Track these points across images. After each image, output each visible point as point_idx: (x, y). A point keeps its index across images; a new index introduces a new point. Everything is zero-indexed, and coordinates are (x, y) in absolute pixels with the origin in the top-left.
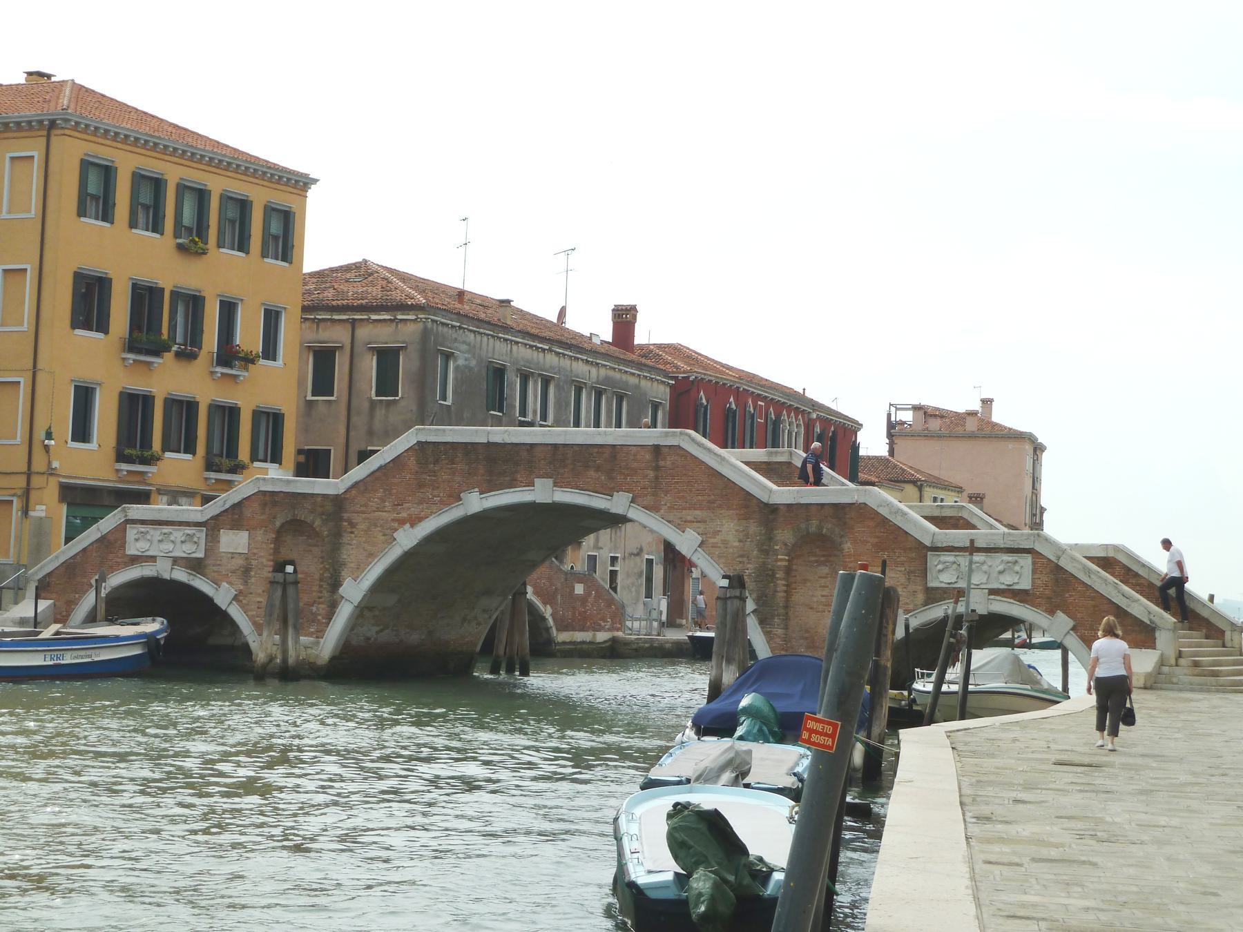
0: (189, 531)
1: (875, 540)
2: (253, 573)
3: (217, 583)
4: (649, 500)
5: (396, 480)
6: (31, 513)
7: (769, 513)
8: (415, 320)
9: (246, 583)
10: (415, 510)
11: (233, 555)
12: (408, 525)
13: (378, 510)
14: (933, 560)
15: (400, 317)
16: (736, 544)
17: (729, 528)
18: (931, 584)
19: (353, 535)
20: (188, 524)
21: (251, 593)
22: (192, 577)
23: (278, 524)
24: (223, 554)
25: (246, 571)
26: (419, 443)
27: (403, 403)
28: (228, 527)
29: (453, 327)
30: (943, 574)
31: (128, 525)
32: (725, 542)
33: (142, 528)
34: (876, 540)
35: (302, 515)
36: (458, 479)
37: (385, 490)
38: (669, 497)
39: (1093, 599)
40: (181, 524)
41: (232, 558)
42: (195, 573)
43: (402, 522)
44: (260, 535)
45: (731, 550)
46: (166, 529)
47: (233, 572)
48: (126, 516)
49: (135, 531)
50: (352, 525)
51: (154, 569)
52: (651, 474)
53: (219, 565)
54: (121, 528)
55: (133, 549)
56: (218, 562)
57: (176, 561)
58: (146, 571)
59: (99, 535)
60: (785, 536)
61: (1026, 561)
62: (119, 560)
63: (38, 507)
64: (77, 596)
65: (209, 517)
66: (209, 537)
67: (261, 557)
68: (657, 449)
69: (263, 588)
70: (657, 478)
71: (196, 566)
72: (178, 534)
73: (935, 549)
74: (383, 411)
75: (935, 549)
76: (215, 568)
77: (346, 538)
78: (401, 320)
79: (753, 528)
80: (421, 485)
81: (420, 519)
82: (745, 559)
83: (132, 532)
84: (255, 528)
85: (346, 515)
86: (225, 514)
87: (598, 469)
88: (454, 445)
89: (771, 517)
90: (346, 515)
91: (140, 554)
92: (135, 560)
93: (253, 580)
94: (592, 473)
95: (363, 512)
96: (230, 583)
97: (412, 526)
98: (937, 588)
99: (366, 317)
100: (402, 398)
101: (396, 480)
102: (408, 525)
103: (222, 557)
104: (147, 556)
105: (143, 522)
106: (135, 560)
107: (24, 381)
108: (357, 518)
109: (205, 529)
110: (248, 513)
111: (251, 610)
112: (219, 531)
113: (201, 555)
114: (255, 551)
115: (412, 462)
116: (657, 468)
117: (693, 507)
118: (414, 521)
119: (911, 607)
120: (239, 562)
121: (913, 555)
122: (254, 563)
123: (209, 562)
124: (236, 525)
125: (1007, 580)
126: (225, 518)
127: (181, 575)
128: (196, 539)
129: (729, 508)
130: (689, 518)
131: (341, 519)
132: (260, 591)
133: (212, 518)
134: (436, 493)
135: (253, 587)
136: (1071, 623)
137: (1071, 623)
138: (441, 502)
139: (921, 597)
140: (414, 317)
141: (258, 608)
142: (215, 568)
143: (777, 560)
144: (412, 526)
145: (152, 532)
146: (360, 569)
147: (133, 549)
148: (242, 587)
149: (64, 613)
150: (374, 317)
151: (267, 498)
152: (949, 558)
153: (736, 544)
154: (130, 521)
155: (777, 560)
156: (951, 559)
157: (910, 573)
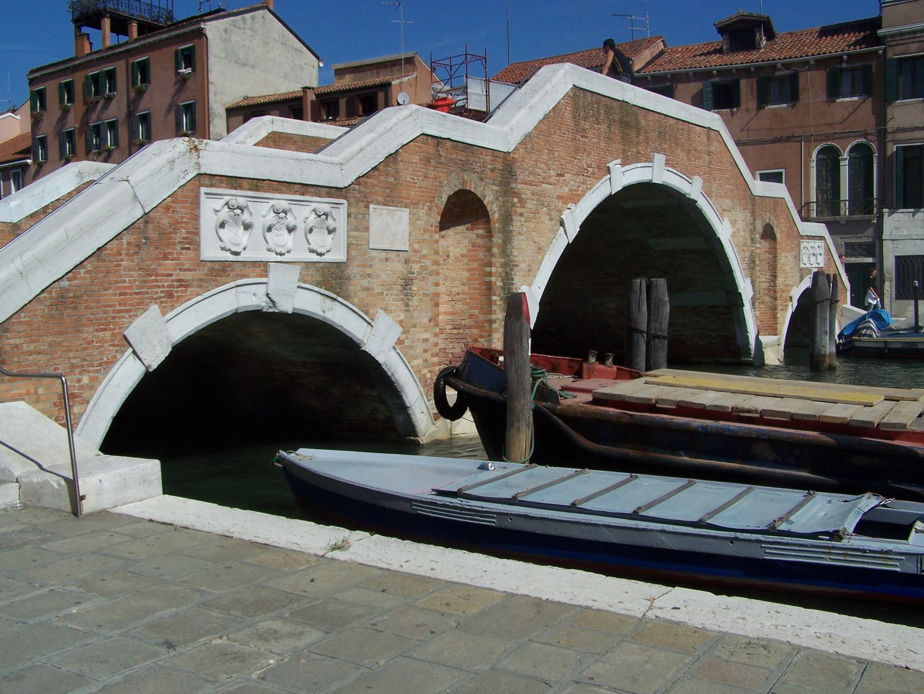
3: (366, 314)
19: (523, 219)
21: (414, 326)
31: (203, 190)
33: (239, 197)
41: (387, 260)
42: (334, 296)
46: (281, 201)
49: (218, 204)
51: (262, 290)
53: (369, 275)
55: (210, 251)
56: (369, 271)
59: (139, 213)
64: (85, 380)
67: (424, 256)
76: (365, 283)
80: (577, 150)
91: (229, 257)
103: (373, 259)
104: (244, 263)
105: (234, 182)
109: (345, 201)
112: (367, 207)
113: (341, 257)
116: (709, 153)
118: (575, 198)
122: (416, 267)
124: (391, 199)
126: (374, 181)
142: (365, 283)
147: (210, 251)
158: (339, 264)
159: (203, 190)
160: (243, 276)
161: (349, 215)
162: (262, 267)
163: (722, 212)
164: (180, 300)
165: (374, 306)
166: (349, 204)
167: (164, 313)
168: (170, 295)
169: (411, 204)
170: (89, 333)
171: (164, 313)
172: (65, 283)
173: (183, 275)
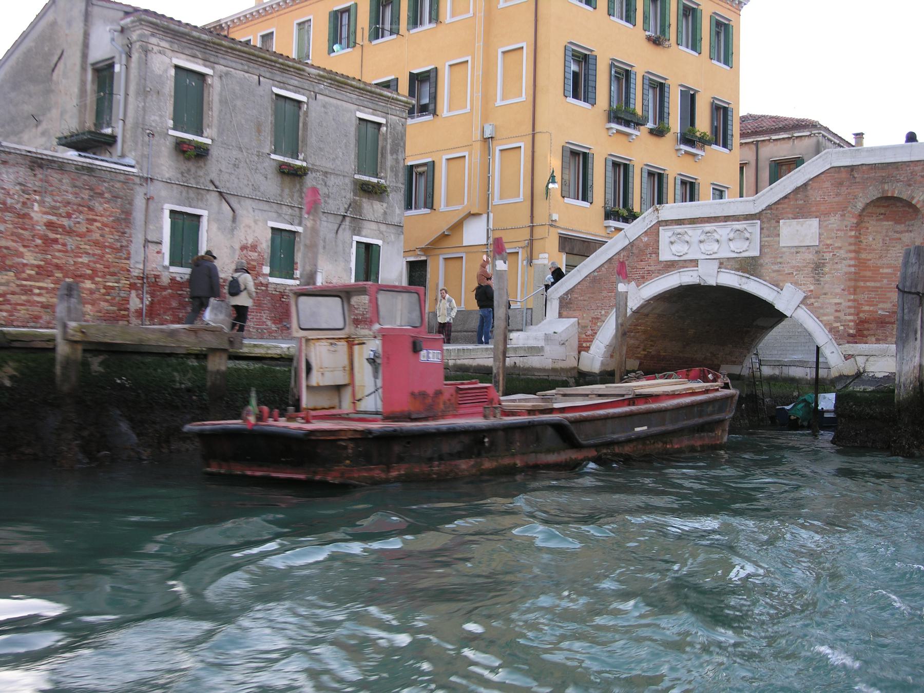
2: (826, 269)
6: (535, 262)
9: (818, 282)
11: (797, 250)
15: (796, 135)
21: (825, 294)
22: (744, 280)
23: (860, 206)
24: (784, 249)
25: (818, 268)
28: (790, 216)
29: (835, 143)
31: (660, 228)
33: (678, 229)
35: (897, 190)
40: (727, 219)
41: (797, 253)
42: (748, 276)
44: (834, 221)
46: (708, 227)
47: (798, 269)
48: (658, 217)
49: (670, 234)
51: (695, 274)
53: (780, 263)
54: (653, 232)
55: (665, 255)
56: (779, 260)
57: (723, 264)
58: (687, 278)
59: (627, 242)
62: (652, 268)
63: (541, 256)
64: (603, 312)
65: (764, 207)
66: (765, 231)
69: (842, 287)
71: (749, 266)
72: (723, 231)
78: (797, 137)
83: (665, 235)
84: (827, 214)
86: (786, 200)
91: (677, 258)
92: (671, 266)
96: (796, 284)
99: (768, 138)
103: (784, 253)
104: (685, 261)
105: (680, 222)
106: (671, 266)
109: (759, 222)
110: (815, 195)
111: (825, 315)
114: (828, 242)
120: (810, 256)
122: (828, 256)
123: (766, 260)
124: (801, 213)
126: (785, 206)
127: (730, 279)
128: (747, 235)
132: (838, 291)
133: (769, 207)
135: (827, 286)
140: (808, 133)
141: (837, 311)
145: (690, 232)
147: (665, 255)
148: (812, 288)
149: (589, 332)
150: (774, 137)
151: (844, 175)
154: (661, 223)
158: (753, 258)
159: (660, 228)
160: (684, 267)
161: (762, 229)
162: (694, 263)
164: (647, 280)
165: (785, 281)
166: (762, 222)
167: (638, 286)
168: (643, 277)
169: (822, 215)
170: (605, 293)
171: (638, 286)
172: (596, 274)
173: (650, 268)
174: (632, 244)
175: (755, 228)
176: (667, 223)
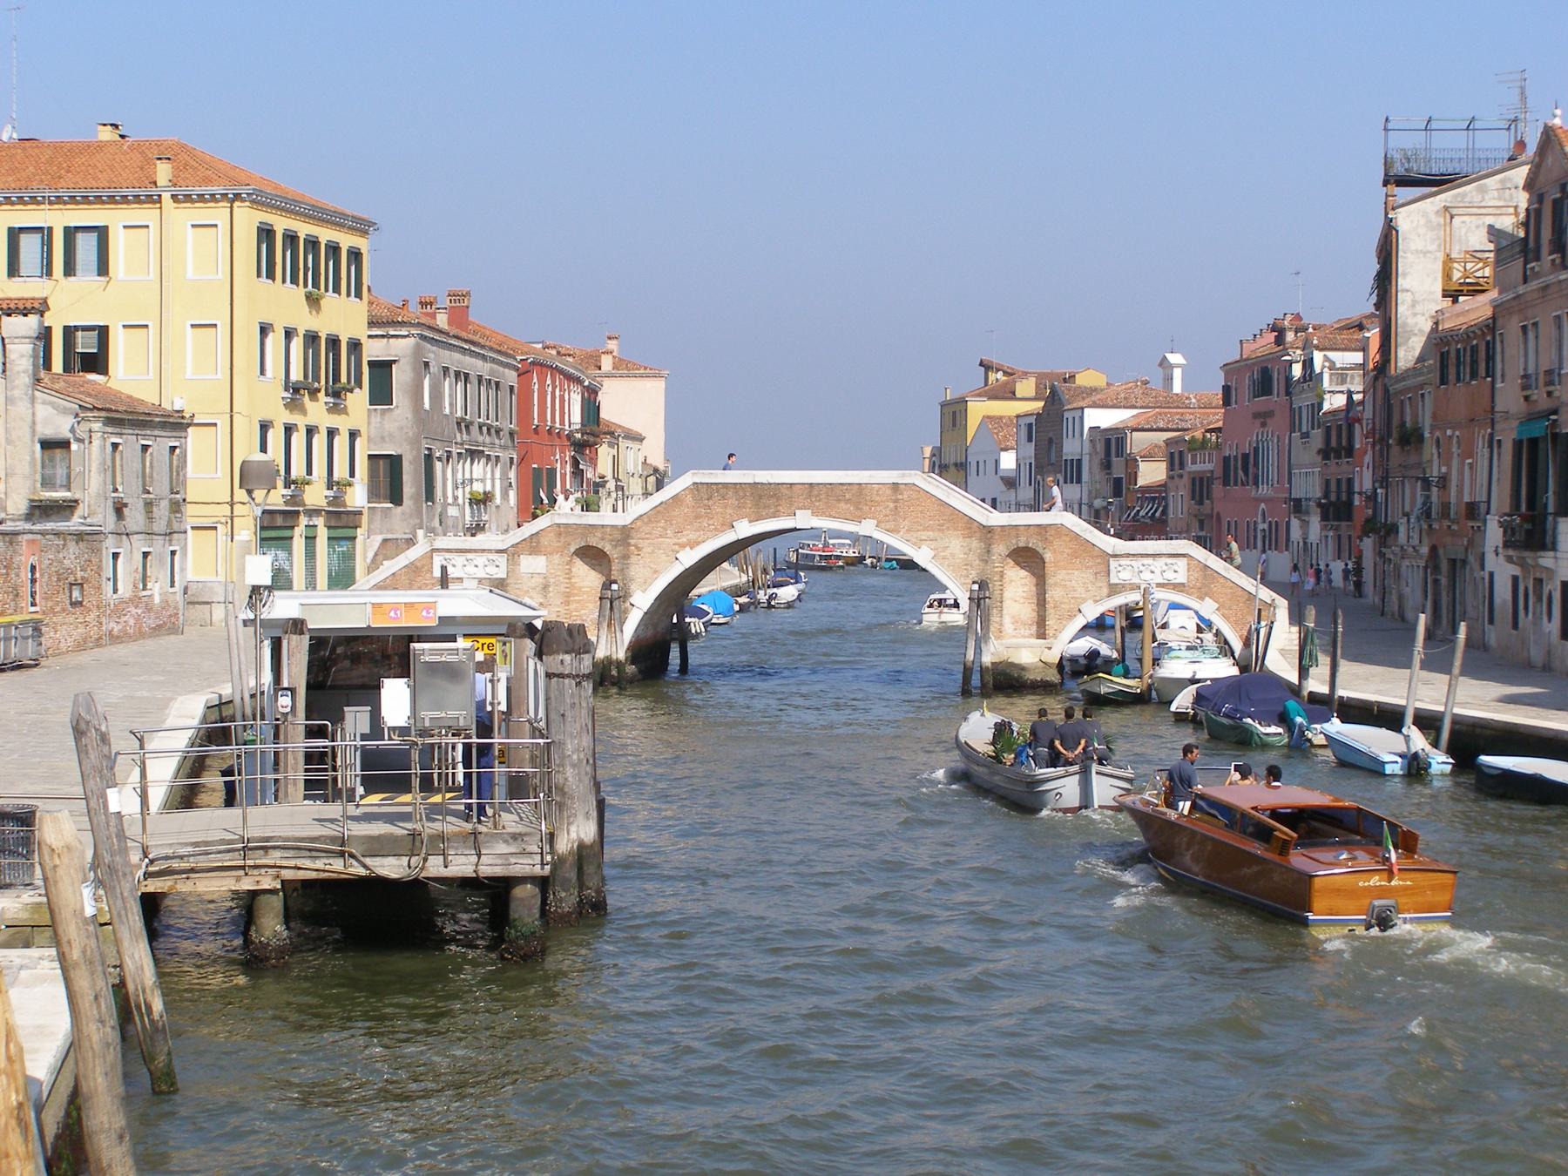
0: (491, 556)
1: (1070, 551)
2: (551, 589)
4: (891, 525)
5: (675, 514)
7: (988, 532)
8: (407, 336)
10: (693, 536)
12: (688, 548)
13: (661, 536)
14: (1113, 563)
16: (962, 556)
17: (956, 545)
18: (1114, 580)
20: (490, 551)
23: (572, 550)
25: (546, 587)
26: (695, 483)
27: (397, 412)
30: (1122, 572)
32: (953, 555)
34: (1070, 551)
36: (729, 511)
37: (666, 521)
38: (906, 522)
39: (1231, 588)
40: (483, 551)
43: (683, 546)
44: (556, 558)
45: (957, 561)
46: (470, 556)
47: (534, 589)
50: (639, 549)
52: (892, 505)
60: (1000, 549)
61: (1182, 564)
68: (895, 486)
70: (896, 508)
72: (481, 560)
73: (1115, 556)
74: (378, 419)
75: (1115, 556)
77: (634, 559)
79: (975, 543)
80: (697, 517)
81: (698, 543)
82: (969, 567)
84: (551, 554)
85: (632, 542)
87: (848, 501)
88: (725, 485)
89: (989, 535)
90: (632, 542)
93: (551, 594)
94: (842, 504)
95: (647, 539)
97: (691, 548)
98: (1117, 584)
100: (397, 407)
101: (675, 514)
102: (688, 548)
105: (448, 551)
107: (223, 423)
108: (641, 543)
110: (545, 541)
113: (505, 576)
115: (689, 499)
116: (896, 501)
117: (926, 529)
118: (693, 545)
119: (1098, 598)
120: (539, 580)
121: (1099, 561)
122: (552, 580)
125: (1170, 575)
129: (956, 529)
130: (924, 538)
131: (629, 545)
133: (512, 546)
134: (711, 522)
136: (1217, 606)
137: (1217, 606)
138: (716, 529)
139: (1105, 591)
140: (407, 333)
143: (994, 567)
144: (691, 548)
146: (646, 585)
152: (1124, 562)
153: (962, 556)
154: (434, 550)
155: (994, 567)
156: (1129, 563)
157: (1096, 574)
163: (917, 544)
174: (412, 563)
175: (502, 560)
176: (438, 550)
